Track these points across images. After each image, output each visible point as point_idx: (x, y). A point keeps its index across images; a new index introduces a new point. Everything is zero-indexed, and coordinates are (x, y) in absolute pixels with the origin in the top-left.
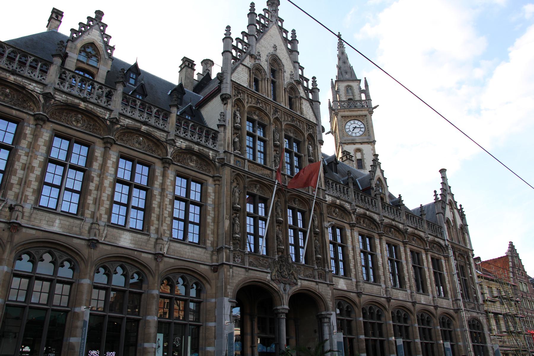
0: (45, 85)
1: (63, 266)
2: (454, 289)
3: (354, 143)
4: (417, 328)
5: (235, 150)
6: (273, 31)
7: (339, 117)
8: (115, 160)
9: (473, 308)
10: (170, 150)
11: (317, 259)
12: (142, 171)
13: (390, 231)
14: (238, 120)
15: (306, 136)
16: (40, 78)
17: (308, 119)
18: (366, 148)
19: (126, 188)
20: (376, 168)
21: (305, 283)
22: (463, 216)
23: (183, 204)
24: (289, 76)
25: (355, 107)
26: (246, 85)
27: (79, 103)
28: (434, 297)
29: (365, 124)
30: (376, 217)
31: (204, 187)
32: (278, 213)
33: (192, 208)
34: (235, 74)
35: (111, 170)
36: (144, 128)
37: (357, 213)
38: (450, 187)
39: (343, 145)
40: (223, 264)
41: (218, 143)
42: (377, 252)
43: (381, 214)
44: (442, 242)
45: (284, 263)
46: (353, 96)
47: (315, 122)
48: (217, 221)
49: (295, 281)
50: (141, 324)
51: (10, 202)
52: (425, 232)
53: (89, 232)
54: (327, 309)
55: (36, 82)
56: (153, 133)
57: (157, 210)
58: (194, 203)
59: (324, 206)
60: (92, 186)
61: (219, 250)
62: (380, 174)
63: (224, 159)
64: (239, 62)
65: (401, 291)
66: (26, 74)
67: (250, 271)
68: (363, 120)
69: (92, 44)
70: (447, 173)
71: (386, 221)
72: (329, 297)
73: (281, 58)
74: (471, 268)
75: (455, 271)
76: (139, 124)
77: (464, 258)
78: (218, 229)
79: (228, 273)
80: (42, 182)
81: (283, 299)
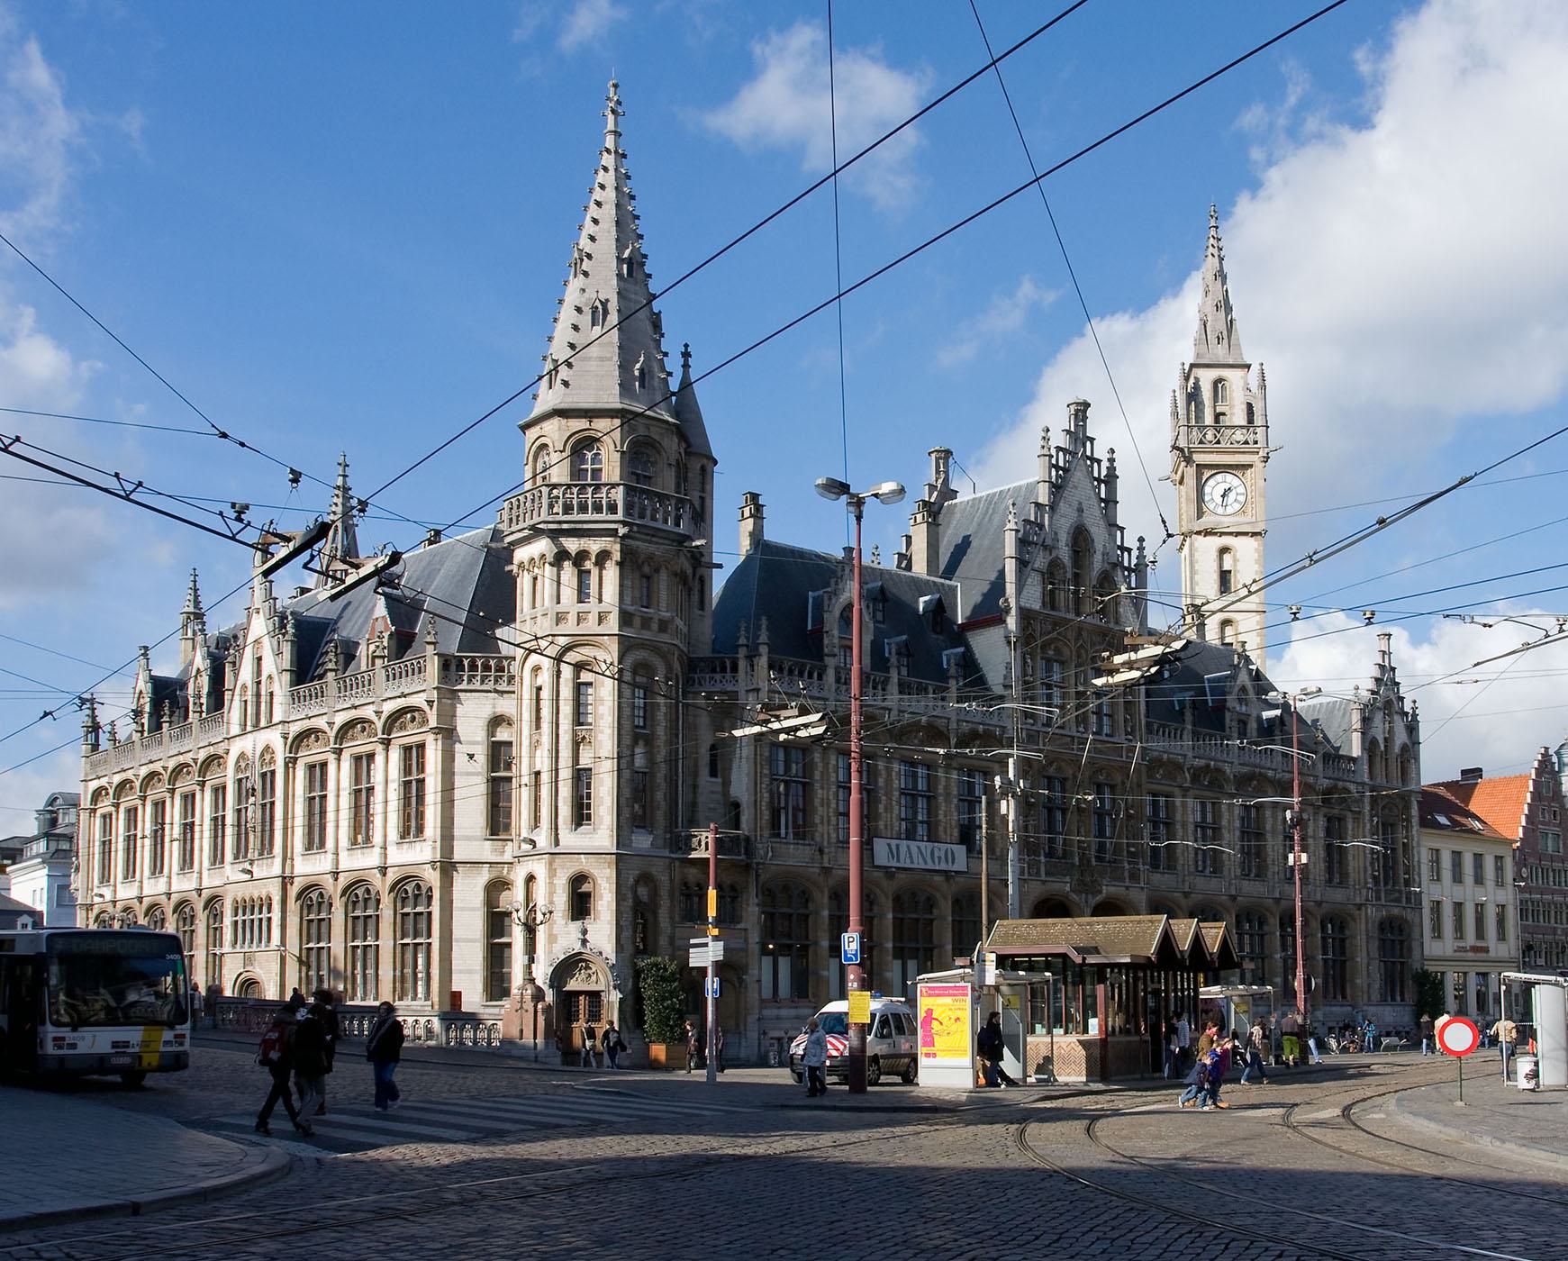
6: (1078, 476)
9: (1398, 900)
21: (1112, 889)
22: (1412, 728)
24: (1100, 557)
26: (1037, 606)
38: (1393, 669)
60: (881, 808)
74: (1408, 828)
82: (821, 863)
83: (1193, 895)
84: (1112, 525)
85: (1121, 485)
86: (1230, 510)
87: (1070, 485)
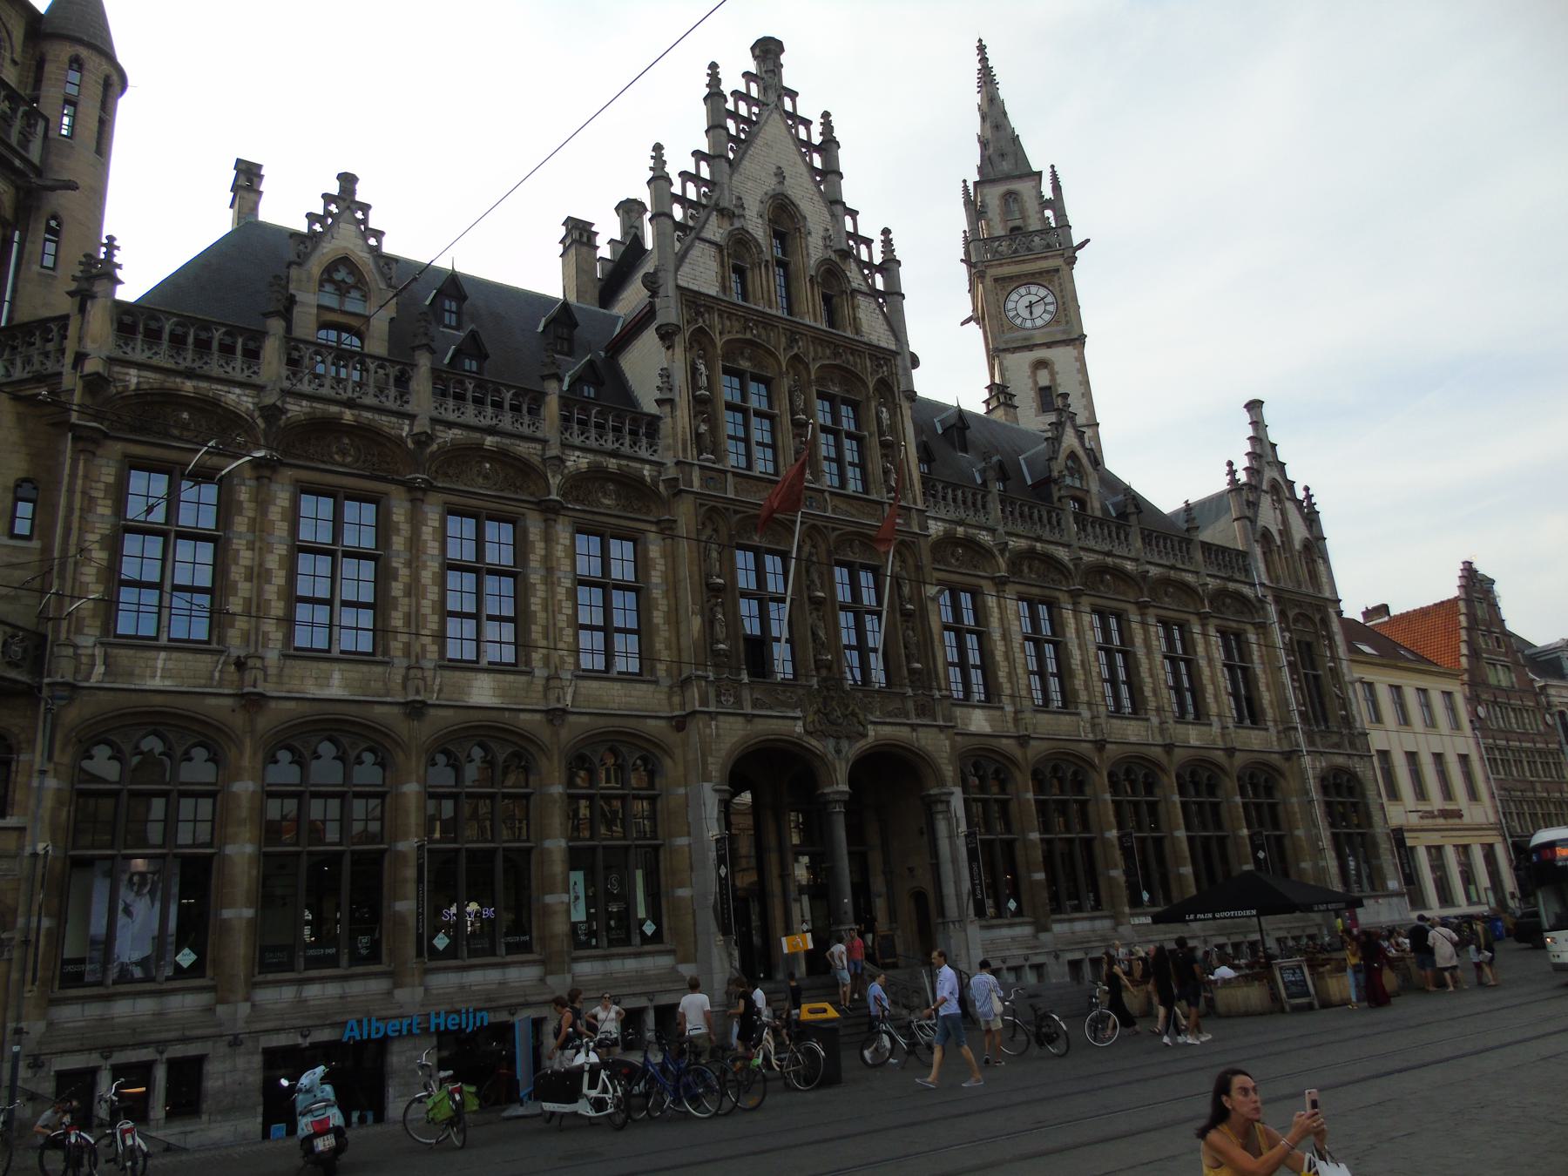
0: (260, 388)
1: (361, 763)
2: (1283, 703)
3: (1030, 348)
4: (1179, 805)
5: (700, 453)
6: (774, 129)
7: (988, 281)
8: (437, 524)
9: (1338, 745)
10: (555, 481)
11: (912, 671)
12: (499, 535)
13: (1102, 581)
14: (703, 381)
15: (871, 386)
16: (246, 373)
17: (875, 342)
18: (1059, 355)
19: (469, 579)
20: (1063, 429)
21: (887, 731)
22: (1311, 517)
23: (597, 593)
25: (1029, 249)
26: (713, 290)
27: (341, 413)
28: (1224, 728)
29: (1058, 295)
30: (1062, 554)
31: (639, 548)
32: (813, 582)
33: (617, 597)
34: (685, 269)
35: (433, 548)
36: (489, 441)
37: (1010, 551)
38: (1274, 446)
39: (1002, 355)
40: (694, 713)
41: (662, 443)
42: (1068, 635)
43: (1076, 544)
44: (1246, 590)
45: (832, 693)
46: (1023, 218)
47: (893, 347)
48: (674, 617)
49: (861, 728)
50: (534, 857)
51: (235, 652)
52: (1197, 573)
53: (405, 687)
54: (941, 782)
55: (241, 385)
56: (511, 449)
57: (541, 616)
58: (622, 587)
59: (925, 548)
60: (397, 588)
61: (685, 683)
62: (1075, 443)
63: (676, 480)
64: (693, 235)
65: (1133, 723)
66: (216, 371)
67: (757, 720)
68: (1050, 282)
69: (345, 261)
70: (1266, 410)
71: (1088, 558)
72: (945, 755)
73: (797, 202)
74: (1332, 646)
75: (1284, 660)
76: (478, 435)
77: (1314, 624)
78: (678, 639)
79: (708, 731)
80: (293, 599)
81: (835, 770)
82: (242, 686)
83: (1033, 743)
84: (835, 205)
85: (842, 154)
86: (1039, 322)
87: (759, 142)
